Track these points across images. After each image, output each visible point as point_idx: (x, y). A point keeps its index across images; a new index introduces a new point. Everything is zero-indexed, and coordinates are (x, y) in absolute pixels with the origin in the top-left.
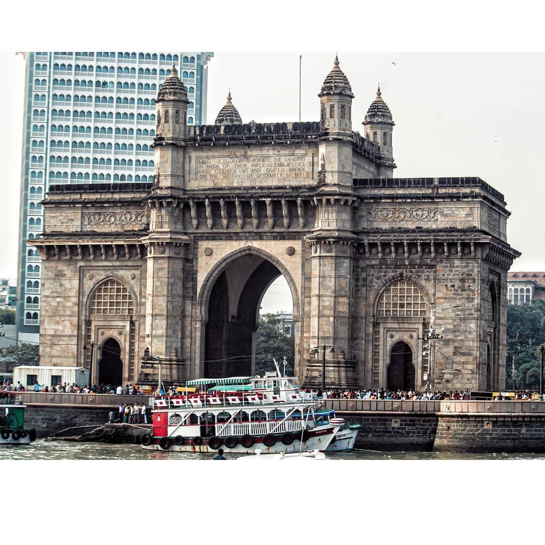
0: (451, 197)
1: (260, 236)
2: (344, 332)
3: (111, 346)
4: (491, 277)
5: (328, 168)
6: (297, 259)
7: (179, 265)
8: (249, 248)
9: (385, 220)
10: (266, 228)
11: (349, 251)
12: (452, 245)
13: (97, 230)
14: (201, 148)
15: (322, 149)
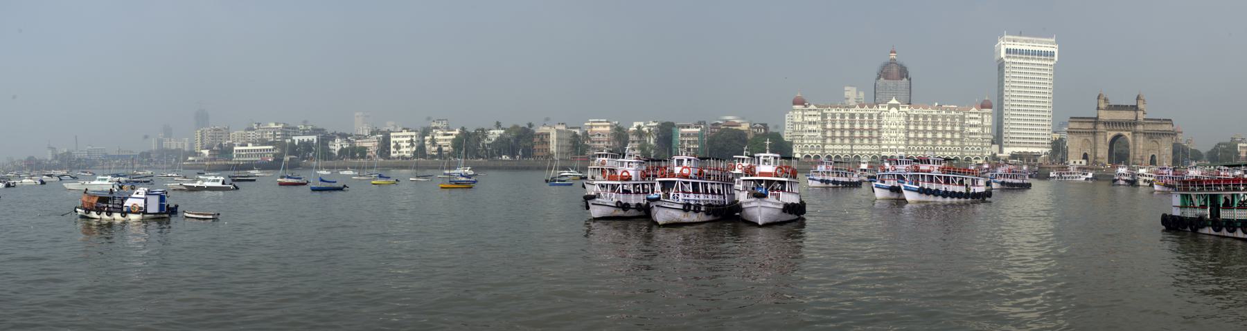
1: (1122, 130)
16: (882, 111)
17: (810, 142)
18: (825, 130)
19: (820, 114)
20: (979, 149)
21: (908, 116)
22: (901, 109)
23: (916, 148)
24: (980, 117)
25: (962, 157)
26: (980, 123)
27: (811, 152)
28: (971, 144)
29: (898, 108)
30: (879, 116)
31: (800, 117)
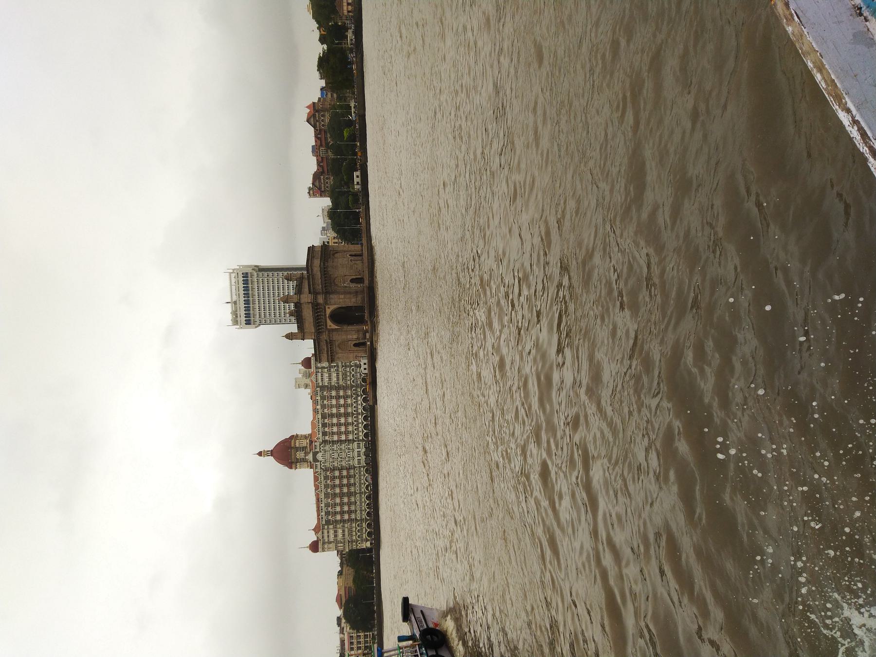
0: (312, 271)
1: (325, 315)
2: (348, 296)
3: (355, 345)
4: (331, 256)
5: (307, 301)
6: (330, 306)
7: (334, 333)
8: (328, 317)
9: (319, 286)
10: (323, 314)
11: (328, 296)
12: (325, 271)
13: (326, 349)
14: (304, 330)
15: (302, 302)
16: (321, 468)
17: (354, 533)
18: (343, 521)
19: (326, 527)
20: (353, 371)
21: (325, 442)
22: (318, 450)
23: (356, 432)
24: (320, 370)
25: (362, 414)
26: (326, 370)
27: (364, 531)
28: (349, 378)
29: (317, 452)
30: (326, 470)
31: (331, 545)
